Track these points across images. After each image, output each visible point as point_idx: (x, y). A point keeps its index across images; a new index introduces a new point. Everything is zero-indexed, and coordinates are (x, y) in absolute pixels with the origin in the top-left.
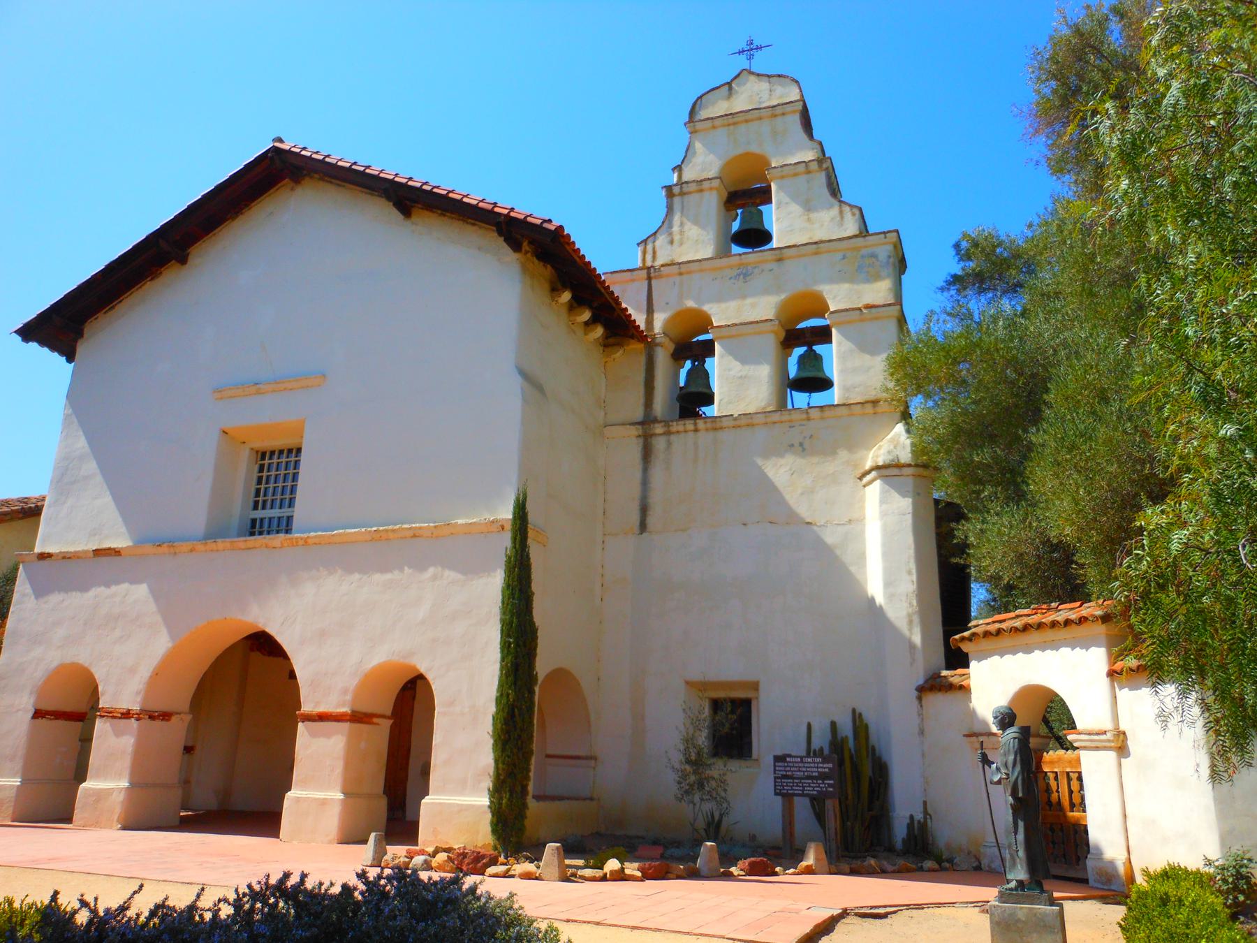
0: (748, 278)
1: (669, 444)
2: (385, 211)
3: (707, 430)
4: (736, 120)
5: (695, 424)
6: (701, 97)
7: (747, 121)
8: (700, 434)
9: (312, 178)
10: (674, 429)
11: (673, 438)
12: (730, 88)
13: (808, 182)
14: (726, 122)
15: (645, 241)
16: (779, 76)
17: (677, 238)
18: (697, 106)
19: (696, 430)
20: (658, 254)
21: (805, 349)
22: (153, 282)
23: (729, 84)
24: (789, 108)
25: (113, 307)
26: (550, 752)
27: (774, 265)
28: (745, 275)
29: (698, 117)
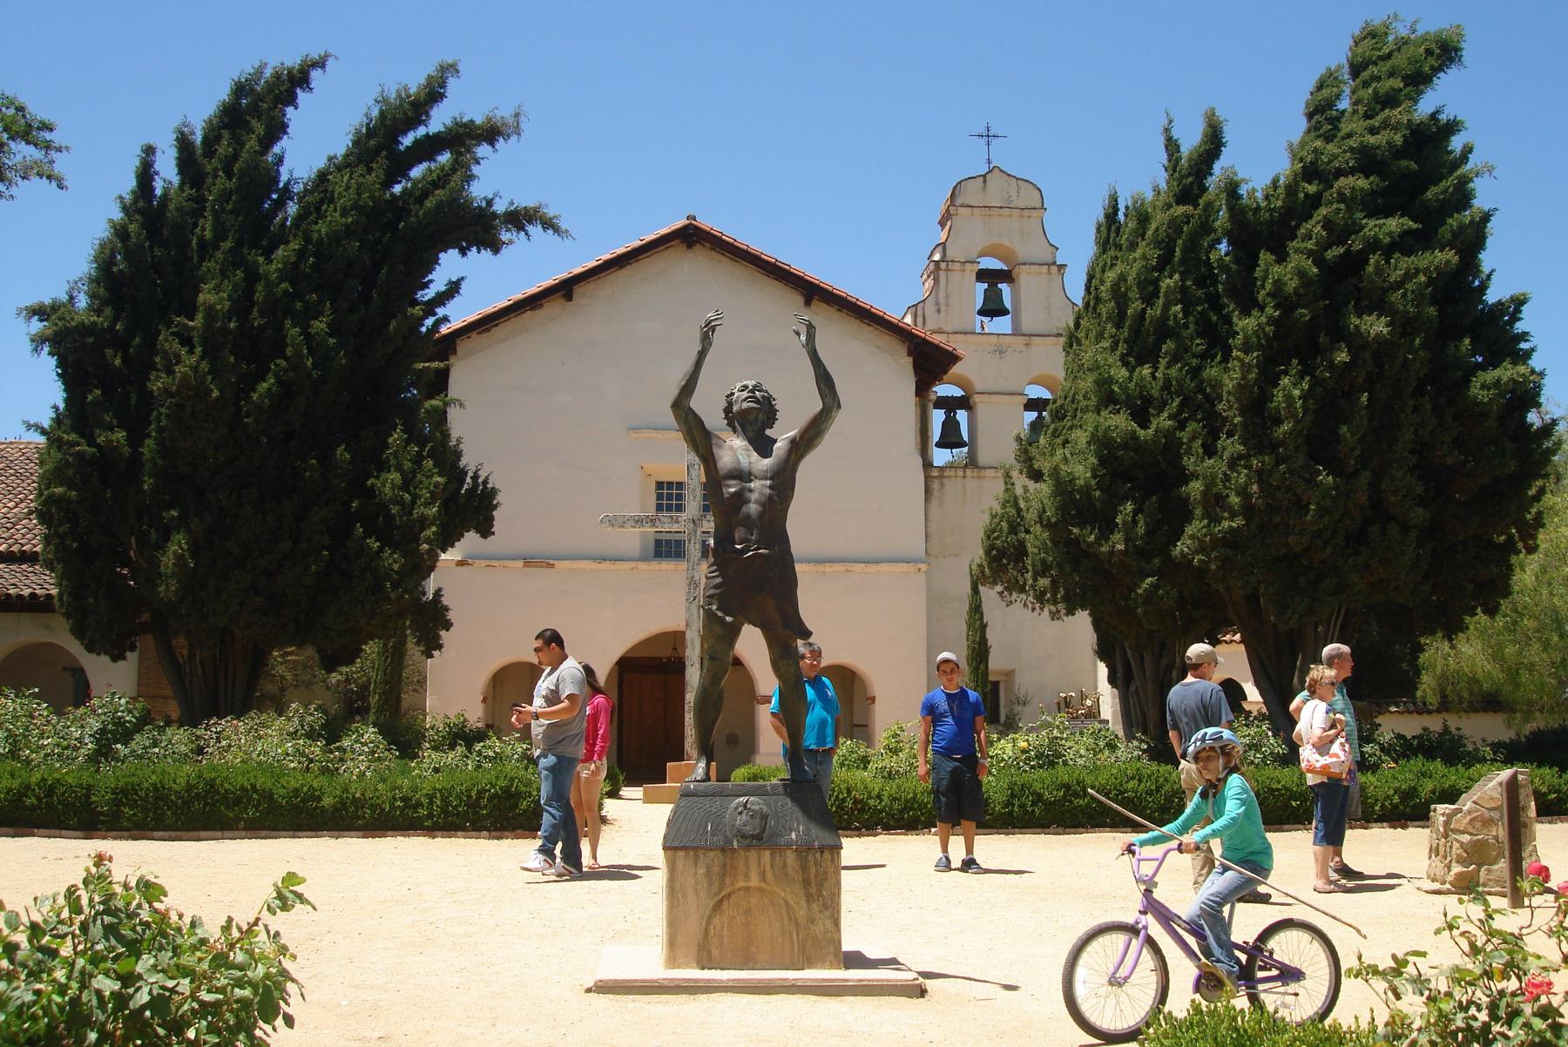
0: (1003, 355)
1: (942, 485)
2: (796, 299)
3: (973, 477)
4: (991, 213)
5: (965, 472)
6: (960, 183)
7: (1000, 215)
8: (966, 480)
9: (703, 246)
10: (946, 474)
11: (945, 480)
12: (985, 182)
13: (1049, 282)
14: (983, 213)
15: (915, 305)
16: (1027, 181)
17: (943, 309)
18: (957, 191)
19: (964, 477)
20: (927, 320)
21: (1035, 414)
22: (533, 312)
23: (984, 176)
24: (1034, 213)
25: (488, 330)
26: (855, 722)
27: (1023, 348)
28: (1001, 352)
29: (959, 201)
